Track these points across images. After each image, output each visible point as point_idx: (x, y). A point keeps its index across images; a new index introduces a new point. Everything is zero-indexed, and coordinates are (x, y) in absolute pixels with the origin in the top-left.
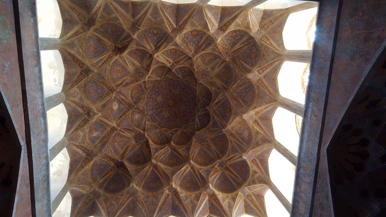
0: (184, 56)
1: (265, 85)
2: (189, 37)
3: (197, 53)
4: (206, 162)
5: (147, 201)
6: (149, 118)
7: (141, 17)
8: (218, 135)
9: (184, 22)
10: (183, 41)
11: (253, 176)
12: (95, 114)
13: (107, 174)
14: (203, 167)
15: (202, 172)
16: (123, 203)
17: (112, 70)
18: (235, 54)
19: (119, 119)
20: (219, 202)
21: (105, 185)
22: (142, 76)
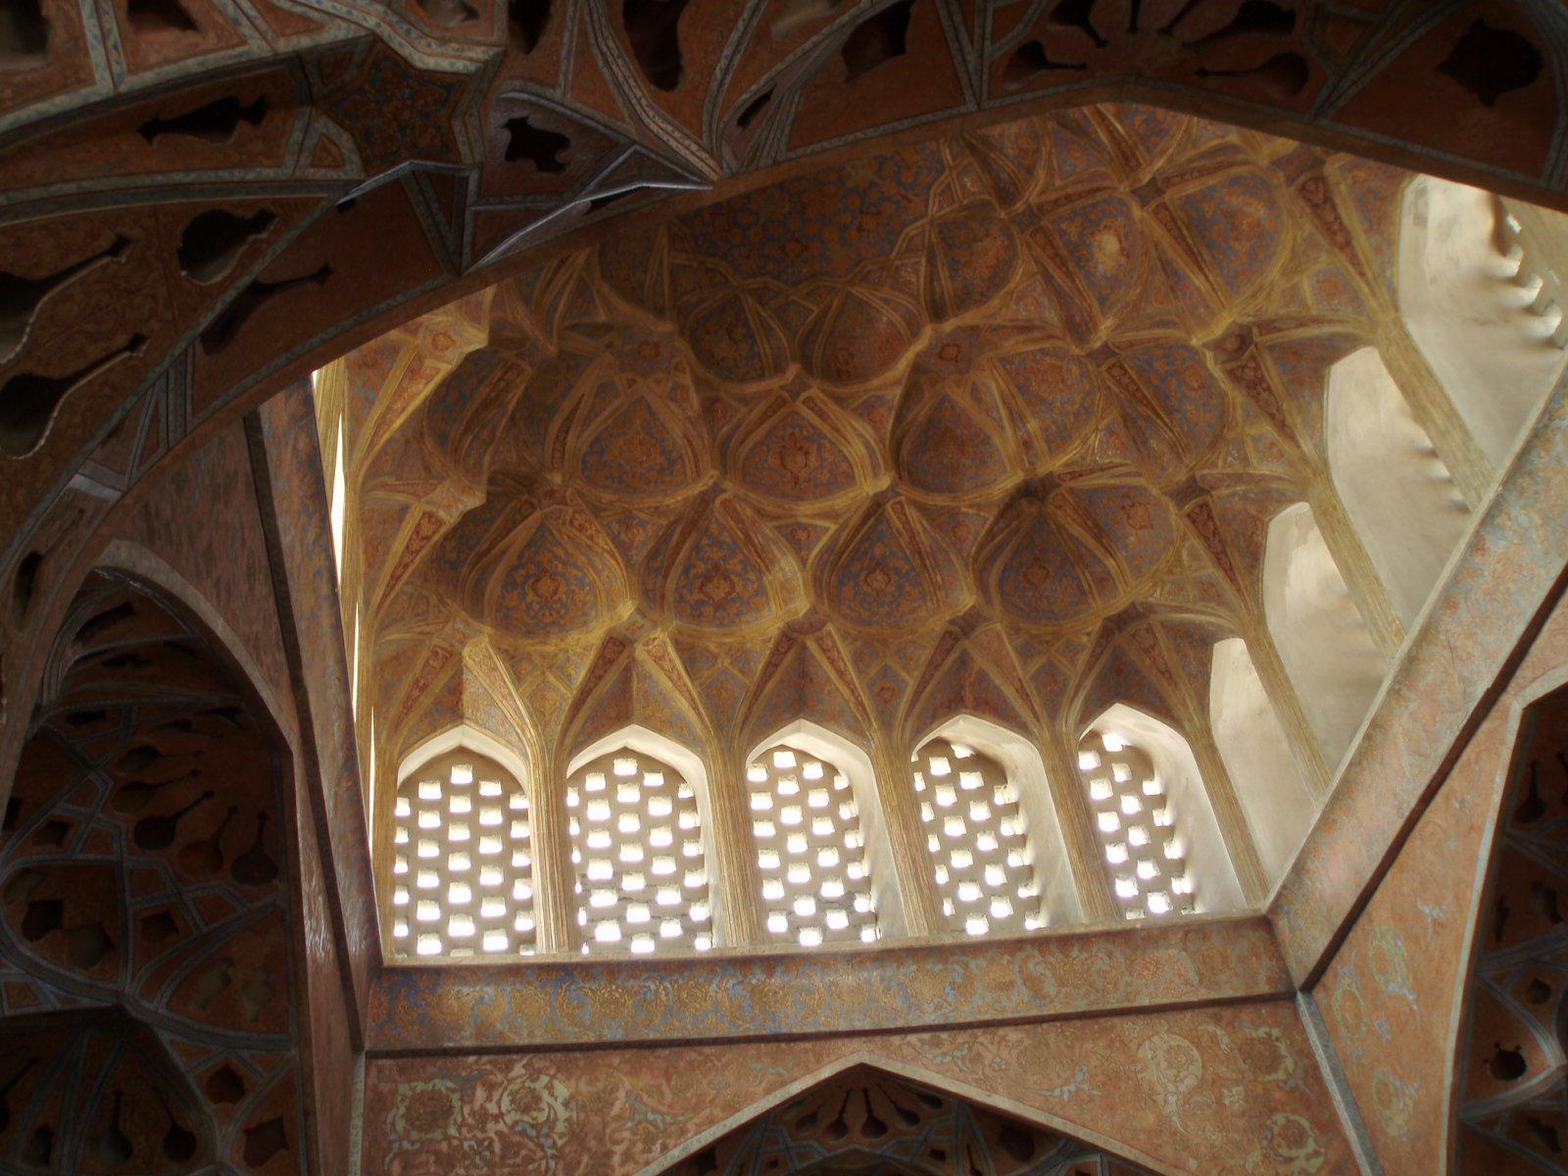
0: (750, 443)
2: (739, 567)
9: (776, 666)
10: (763, 561)
12: (1218, 346)
18: (526, 501)
19: (1105, 188)
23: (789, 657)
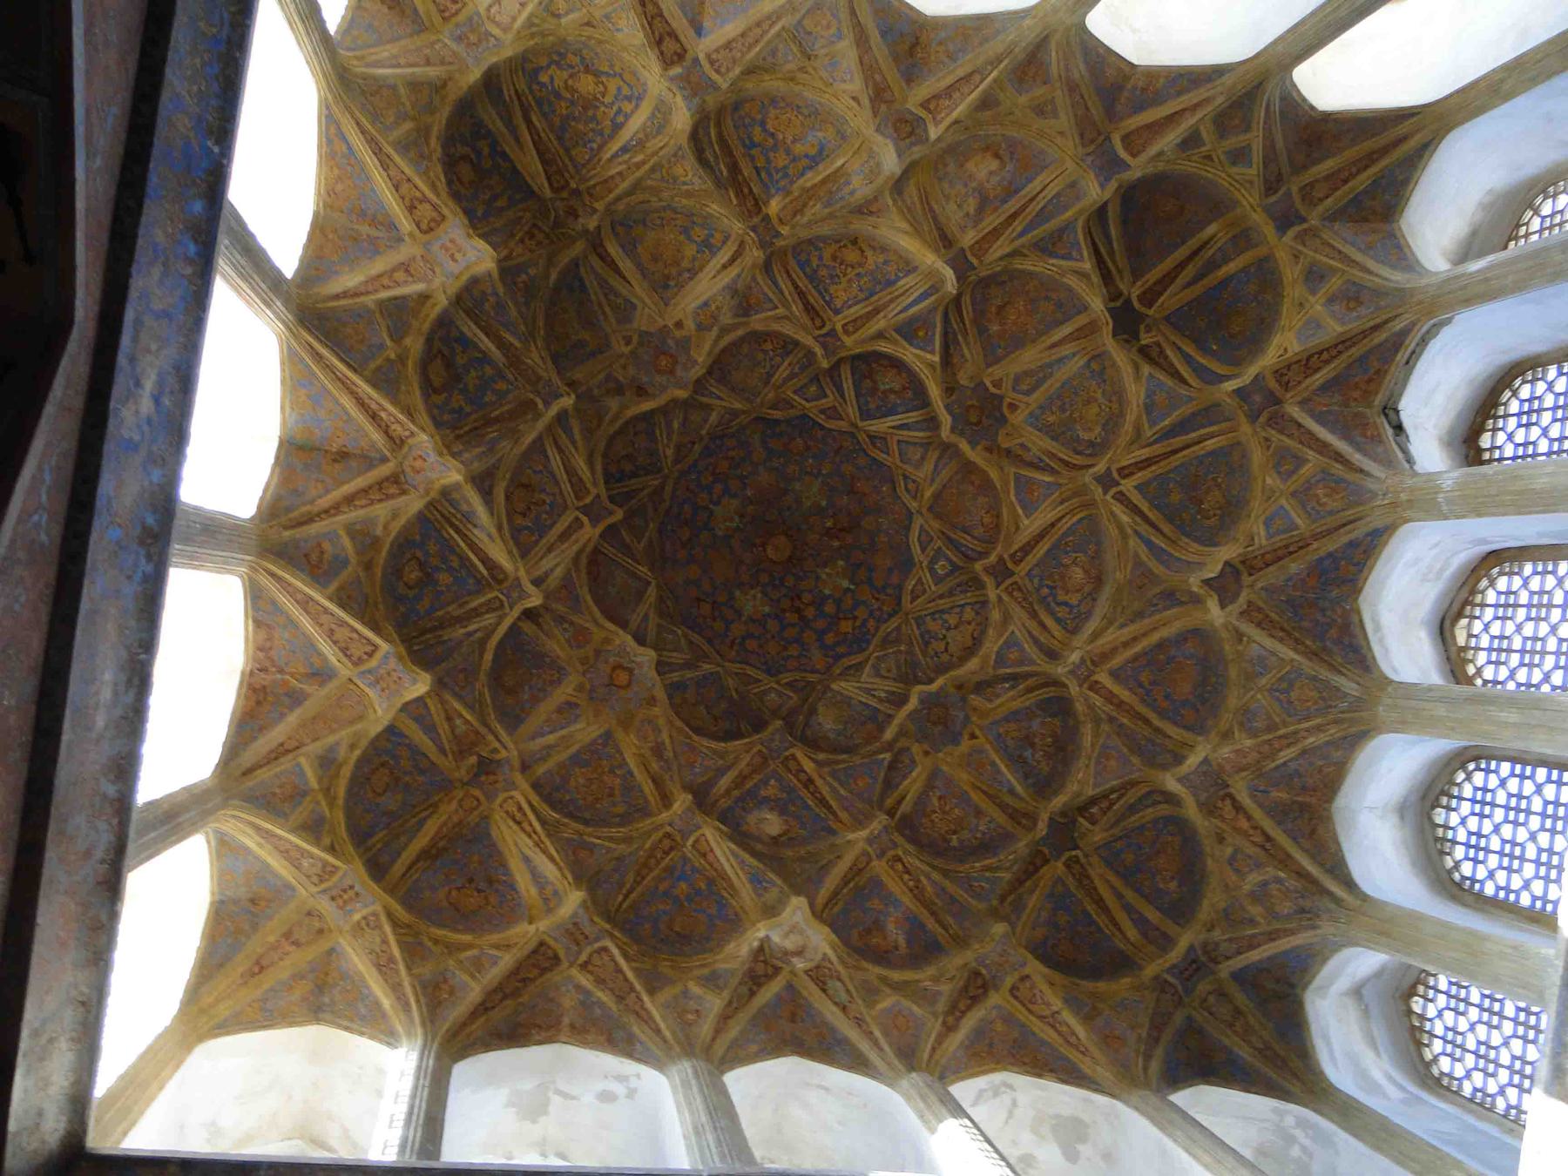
0: (551, 452)
1: (743, 35)
2: (456, 405)
3: (540, 378)
4: (1101, 400)
5: (1270, 718)
6: (846, 662)
7: (331, 634)
8: (975, 321)
11: (1209, 158)
13: (1099, 902)
14: (1130, 417)
15: (1153, 423)
16: (1259, 839)
17: (587, 815)
18: (567, 183)
19: (835, 814)
20: (1320, 353)
21: (1152, 915)
22: (631, 671)
23: (376, 436)
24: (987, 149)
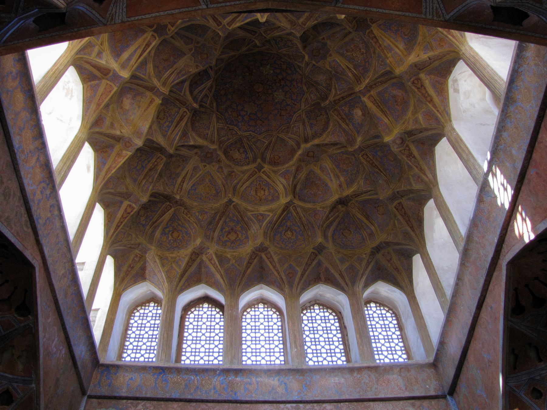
0: (244, 187)
2: (240, 229)
3: (226, 205)
6: (298, 70)
24: (122, 108)
